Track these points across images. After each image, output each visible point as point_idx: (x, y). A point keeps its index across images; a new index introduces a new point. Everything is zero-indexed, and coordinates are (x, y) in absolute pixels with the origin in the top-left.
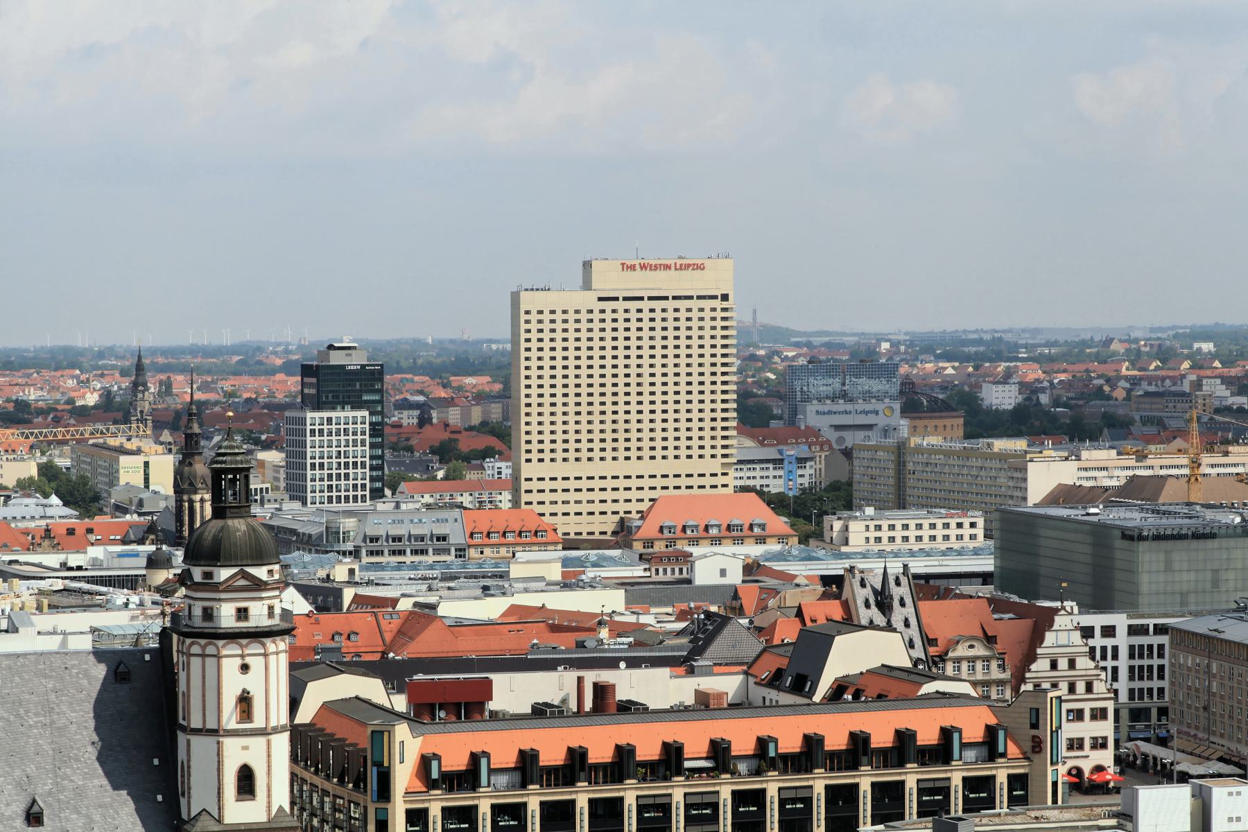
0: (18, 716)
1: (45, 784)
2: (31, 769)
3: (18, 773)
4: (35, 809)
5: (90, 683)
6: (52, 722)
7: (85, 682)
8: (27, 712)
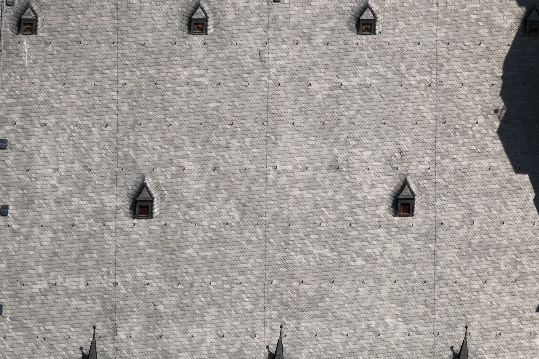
0: (398, 72)
1: (420, 163)
2: (406, 143)
3: (389, 146)
4: (406, 193)
5: (491, 34)
6: (439, 83)
7: (485, 32)
8: (409, 67)
